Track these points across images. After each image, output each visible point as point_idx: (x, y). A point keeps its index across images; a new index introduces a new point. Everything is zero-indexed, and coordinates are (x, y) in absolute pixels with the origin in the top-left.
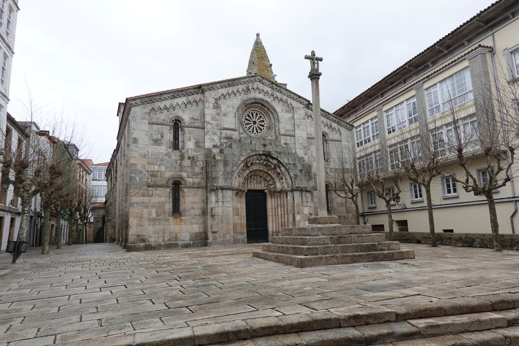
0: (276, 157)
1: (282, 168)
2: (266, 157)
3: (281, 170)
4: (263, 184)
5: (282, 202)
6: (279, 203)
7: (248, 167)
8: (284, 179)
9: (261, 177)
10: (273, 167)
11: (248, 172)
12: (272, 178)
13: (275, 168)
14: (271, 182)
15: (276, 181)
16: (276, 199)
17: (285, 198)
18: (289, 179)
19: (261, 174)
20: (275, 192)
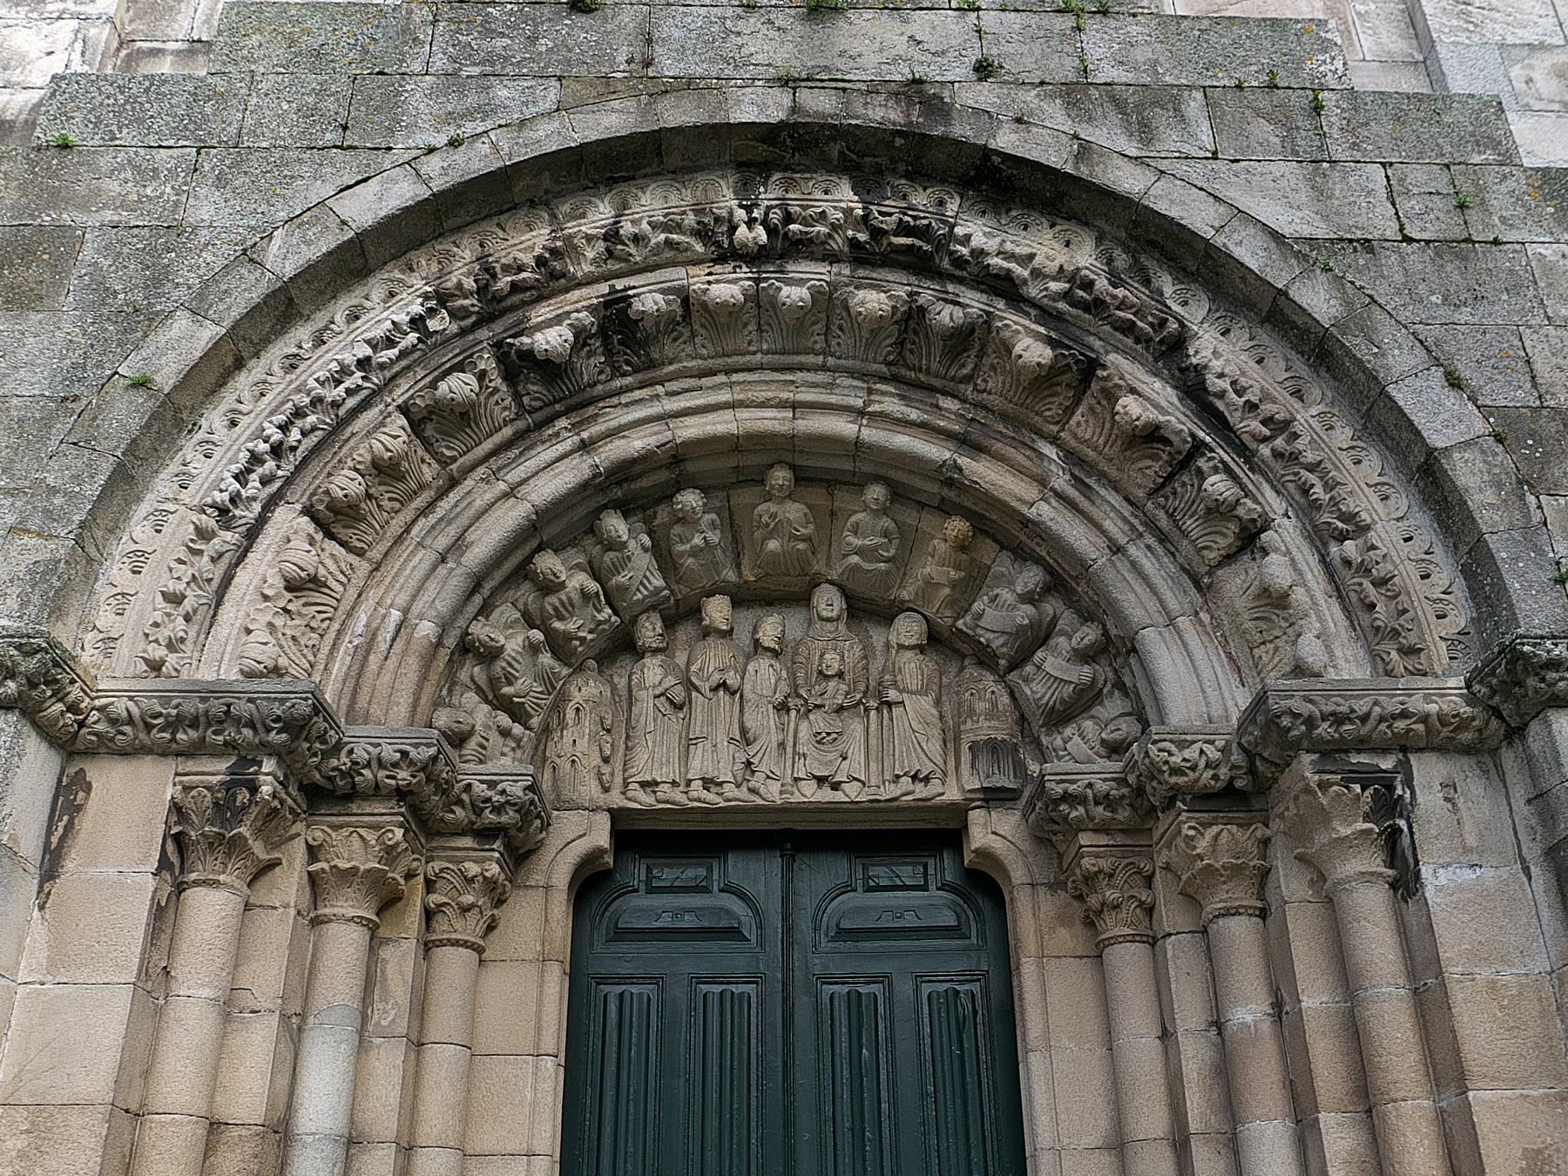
0: (1056, 157)
1: (1220, 351)
2: (866, 185)
3: (1193, 386)
4: (917, 711)
5: (1315, 999)
6: (1249, 1012)
7: (549, 391)
8: (1286, 533)
9: (886, 614)
10: (1032, 350)
11: (553, 472)
12: (1065, 580)
13: (1079, 375)
14: (1055, 671)
15: (1134, 602)
16: (1180, 954)
17: (1370, 909)
18: (1394, 527)
19: (864, 530)
20: (1145, 802)
